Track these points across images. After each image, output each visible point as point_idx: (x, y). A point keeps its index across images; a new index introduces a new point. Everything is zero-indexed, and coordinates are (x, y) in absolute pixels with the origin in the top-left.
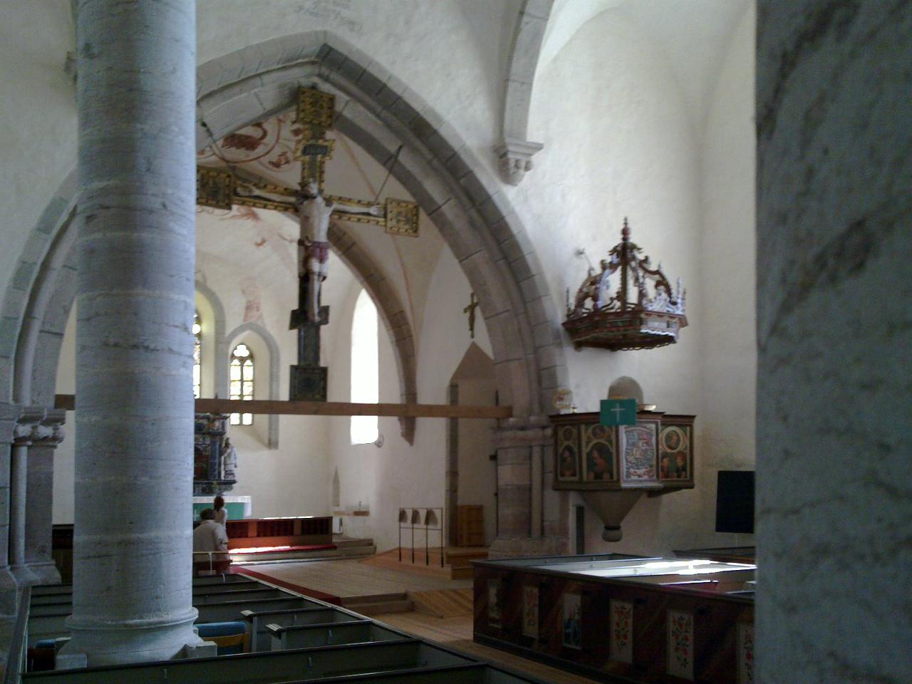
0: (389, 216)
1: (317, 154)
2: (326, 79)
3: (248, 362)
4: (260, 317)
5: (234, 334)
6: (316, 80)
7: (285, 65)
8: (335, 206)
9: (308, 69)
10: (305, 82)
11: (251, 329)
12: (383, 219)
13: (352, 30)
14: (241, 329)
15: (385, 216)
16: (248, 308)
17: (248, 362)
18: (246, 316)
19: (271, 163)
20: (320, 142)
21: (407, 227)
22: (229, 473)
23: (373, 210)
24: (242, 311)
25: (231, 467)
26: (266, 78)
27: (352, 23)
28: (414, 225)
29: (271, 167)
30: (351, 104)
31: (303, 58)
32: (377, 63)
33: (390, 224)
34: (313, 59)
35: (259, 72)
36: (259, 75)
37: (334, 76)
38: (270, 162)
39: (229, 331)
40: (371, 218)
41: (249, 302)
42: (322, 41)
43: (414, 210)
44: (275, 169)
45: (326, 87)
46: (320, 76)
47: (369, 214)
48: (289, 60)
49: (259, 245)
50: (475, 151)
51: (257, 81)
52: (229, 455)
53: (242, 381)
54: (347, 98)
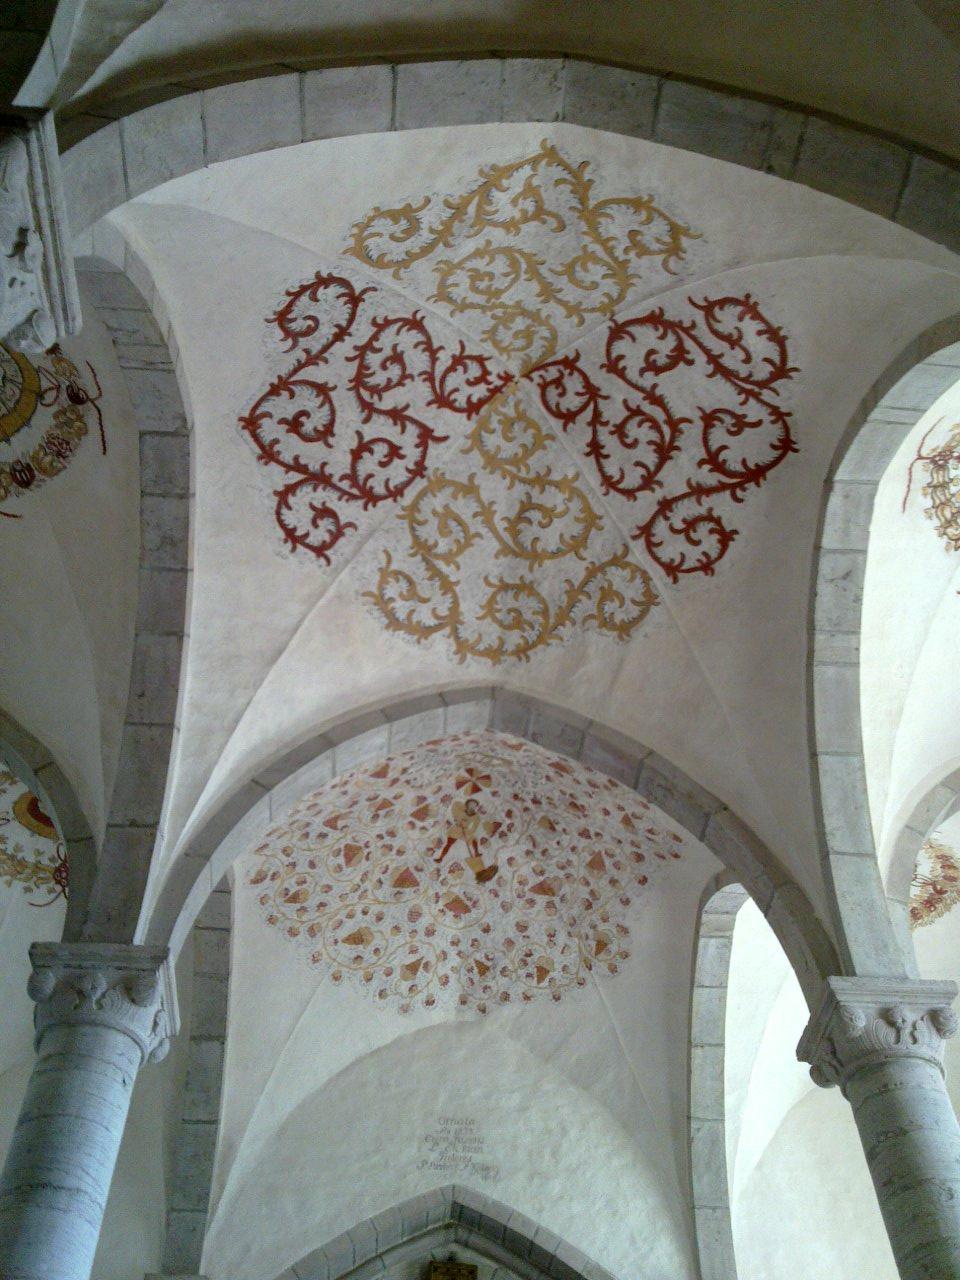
2: (466, 1245)
6: (454, 1247)
7: (411, 1237)
9: (441, 1236)
10: (440, 1253)
13: (485, 1178)
26: (388, 1259)
27: (486, 1169)
30: (501, 1273)
31: (436, 1221)
32: (520, 1215)
34: (447, 1221)
35: (380, 1251)
36: (380, 1256)
37: (474, 1239)
42: (450, 1199)
45: (466, 1256)
46: (456, 1241)
48: (417, 1229)
51: (379, 1263)
54: (494, 1265)
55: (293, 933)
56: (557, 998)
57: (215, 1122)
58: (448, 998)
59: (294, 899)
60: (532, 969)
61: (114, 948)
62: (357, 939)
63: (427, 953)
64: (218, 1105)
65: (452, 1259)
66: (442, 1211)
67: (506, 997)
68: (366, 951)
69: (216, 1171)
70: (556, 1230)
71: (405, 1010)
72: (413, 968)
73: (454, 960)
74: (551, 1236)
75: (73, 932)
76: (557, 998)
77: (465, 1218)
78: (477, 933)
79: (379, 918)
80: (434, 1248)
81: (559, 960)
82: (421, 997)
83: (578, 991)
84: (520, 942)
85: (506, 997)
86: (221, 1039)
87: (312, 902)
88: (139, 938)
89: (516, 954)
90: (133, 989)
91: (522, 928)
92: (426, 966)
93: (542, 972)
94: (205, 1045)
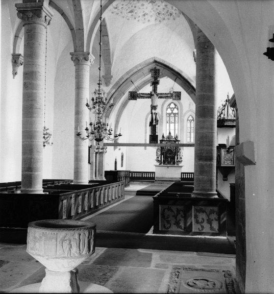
3: (192, 122)
5: (185, 114)
6: (157, 66)
8: (159, 96)
14: (188, 111)
15: (172, 96)
16: (190, 105)
17: (192, 122)
22: (181, 158)
23: (169, 95)
25: (181, 156)
45: (158, 68)
50: (192, 78)
52: (180, 153)
53: (191, 128)
55: (117, 14)
56: (174, 19)
57: (109, 49)
58: (153, 19)
59: (116, 8)
60: (169, 14)
61: (81, 53)
62: (131, 12)
63: (146, 12)
64: (109, 46)
65: (155, 68)
66: (152, 61)
67: (164, 19)
68: (134, 14)
69: (111, 56)
71: (144, 23)
72: (144, 15)
73: (153, 12)
75: (75, 51)
76: (174, 19)
77: (155, 62)
78: (157, 7)
79: (135, 7)
80: (153, 66)
81: (173, 11)
82: (147, 20)
83: (178, 18)
84: (166, 9)
85: (164, 19)
86: (107, 36)
87: (120, 8)
88: (85, 51)
89: (165, 11)
90: (86, 59)
91: (166, 6)
92: (147, 14)
93: (171, 14)
94: (105, 37)
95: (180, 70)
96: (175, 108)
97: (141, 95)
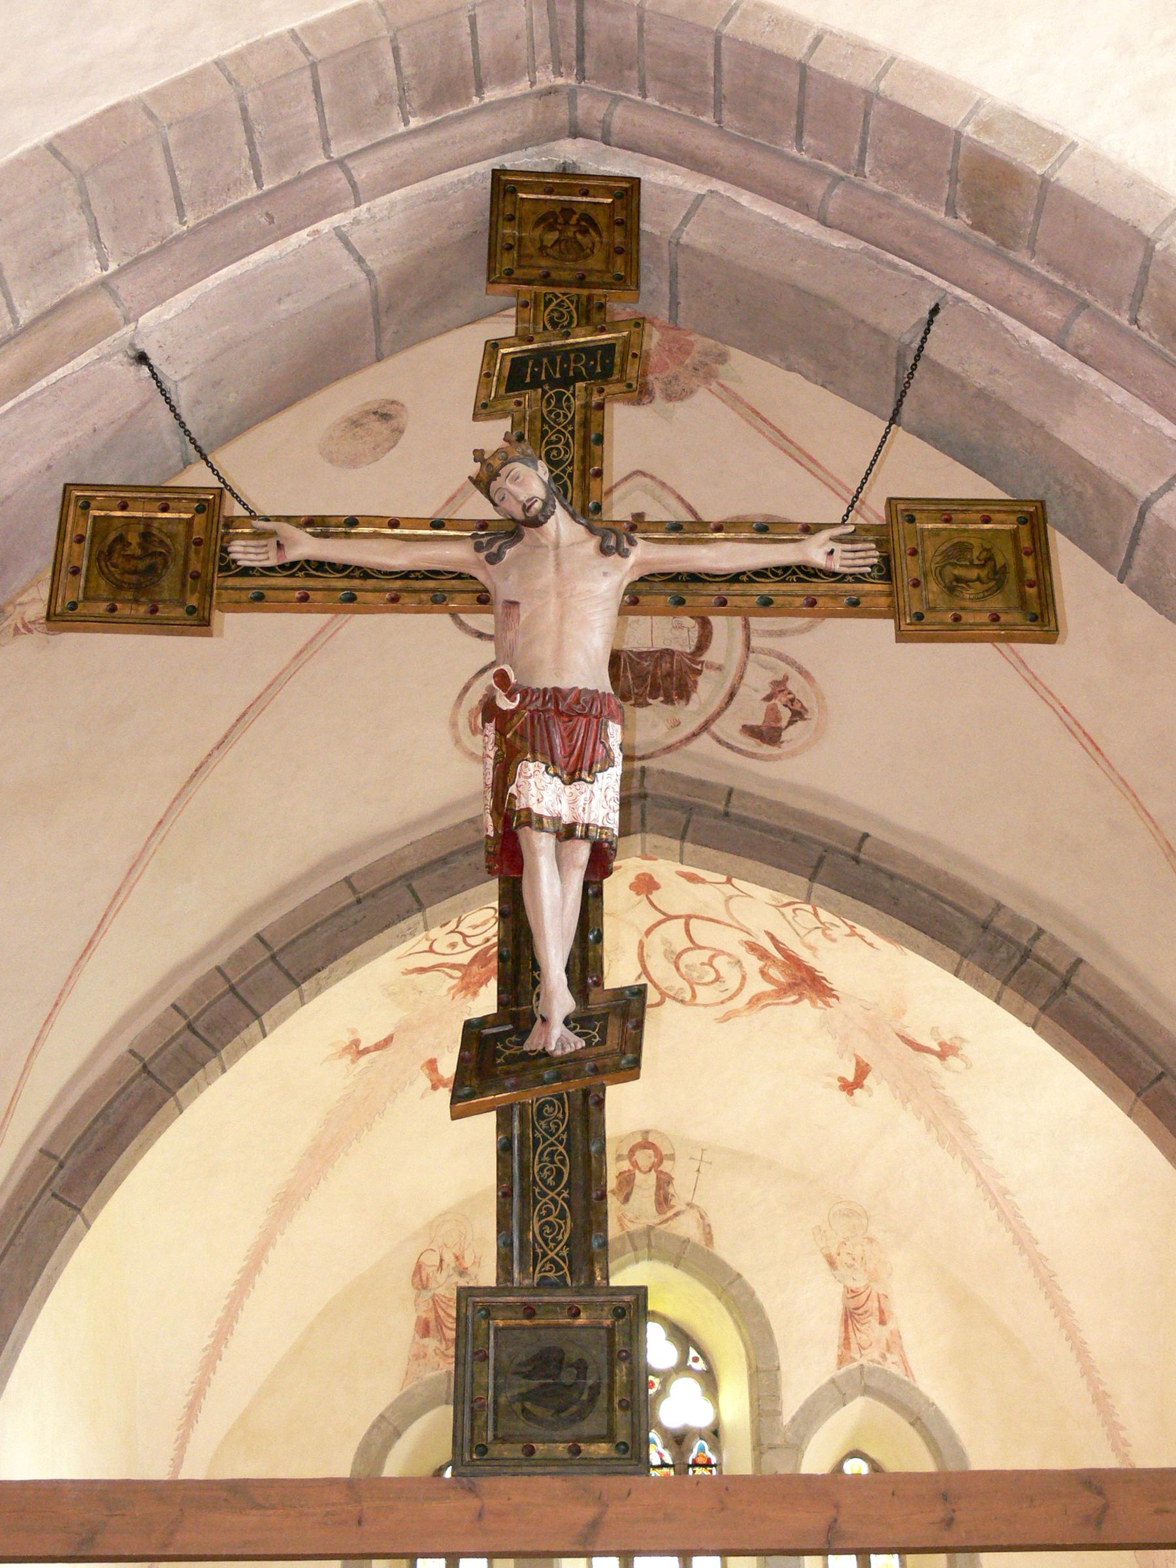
0: (908, 568)
1: (567, 382)
4: (894, 1344)
11: (867, 1390)
12: (882, 587)
16: (850, 1317)
18: (846, 1342)
19: (751, 731)
20: (582, 338)
21: (995, 603)
24: (834, 1329)
28: (1032, 591)
29: (750, 744)
33: (912, 601)
38: (744, 726)
39: (792, 1402)
40: (821, 587)
41: (852, 1293)
43: (1024, 531)
44: (766, 749)
47: (805, 572)
49: (849, 1087)
70: (876, 37)
74: (863, 49)
95: (1017, 121)
96: (682, 1367)
97: (305, 547)
